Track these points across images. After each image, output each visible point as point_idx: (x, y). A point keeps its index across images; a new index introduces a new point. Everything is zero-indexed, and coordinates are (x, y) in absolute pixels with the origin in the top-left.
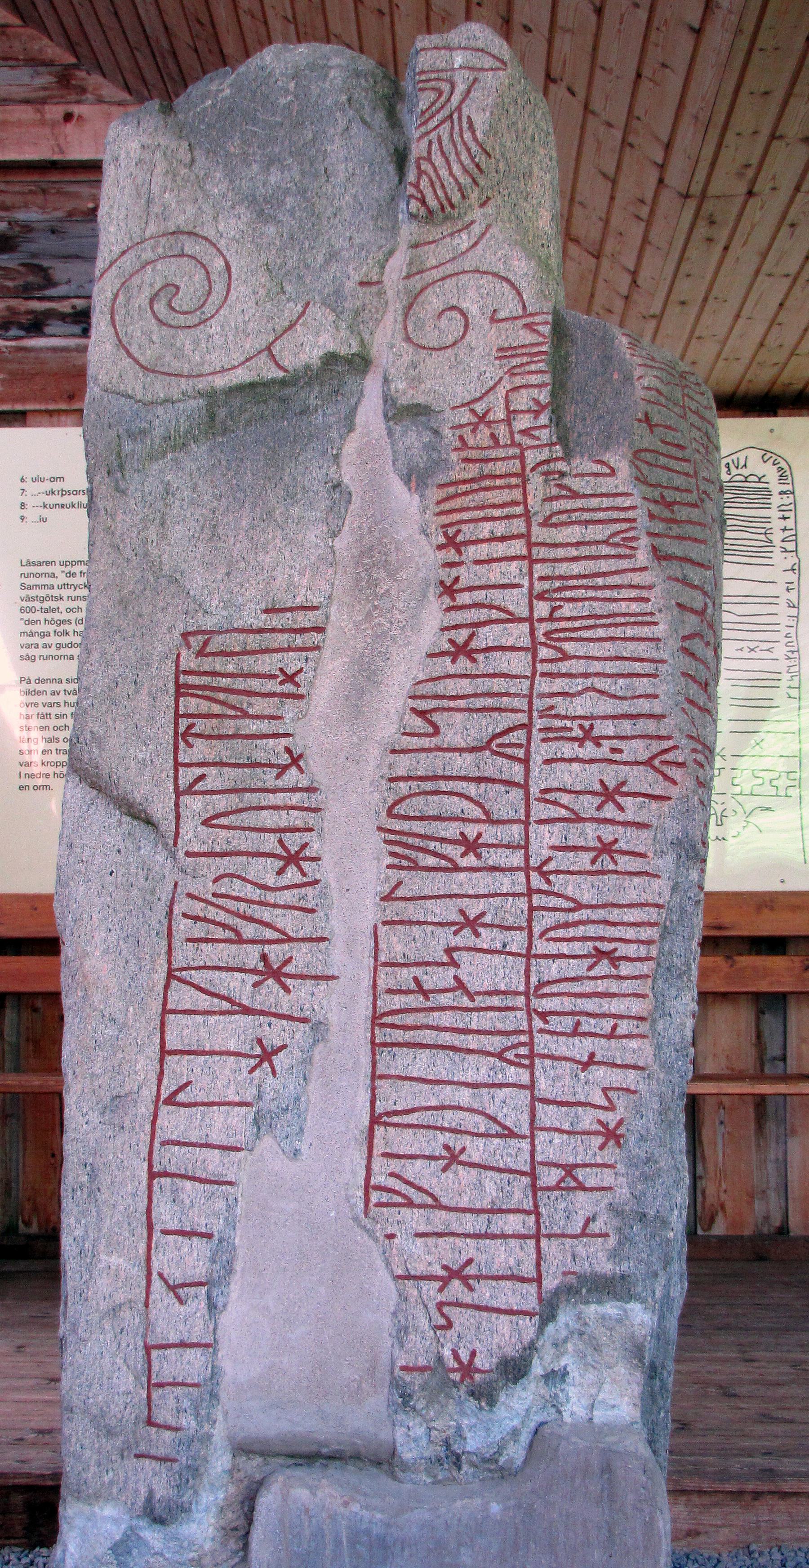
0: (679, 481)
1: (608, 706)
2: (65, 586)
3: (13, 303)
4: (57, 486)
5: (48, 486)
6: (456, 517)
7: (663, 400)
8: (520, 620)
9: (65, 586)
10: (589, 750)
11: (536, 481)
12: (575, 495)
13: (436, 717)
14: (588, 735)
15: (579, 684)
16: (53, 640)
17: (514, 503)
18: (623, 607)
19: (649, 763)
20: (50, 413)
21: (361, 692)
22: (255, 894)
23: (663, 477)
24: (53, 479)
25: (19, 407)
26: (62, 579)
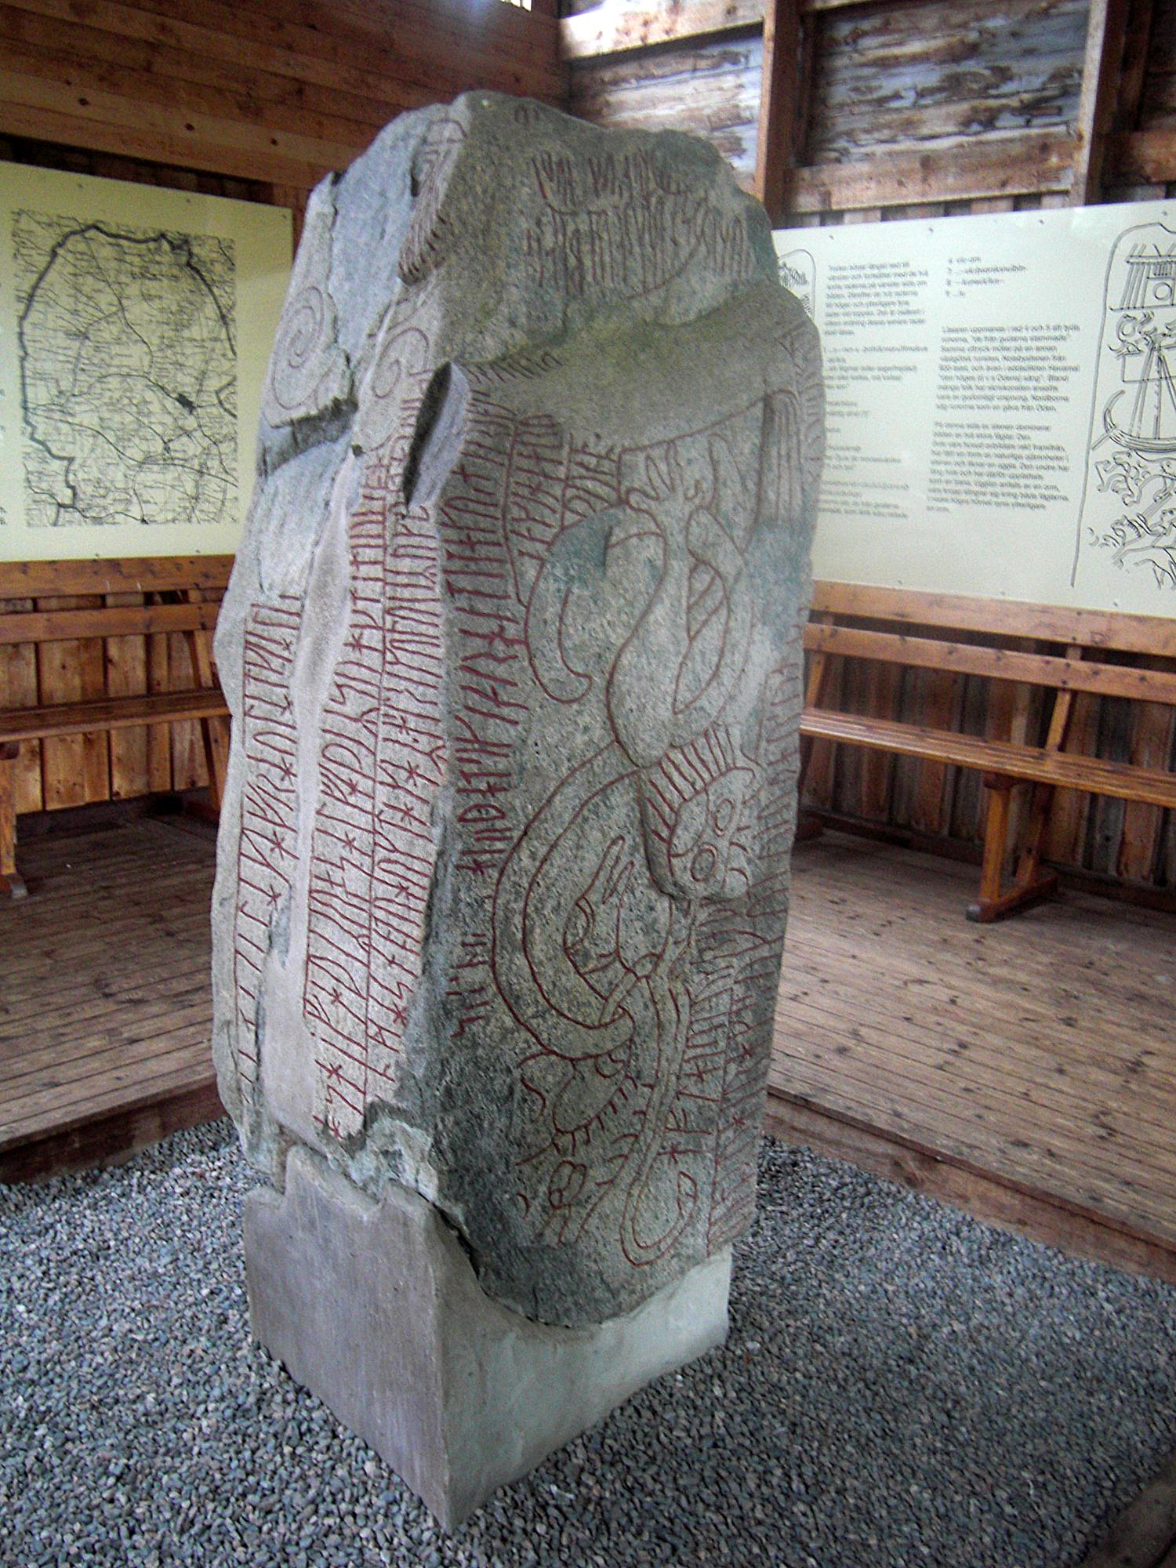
0: (484, 523)
1: (415, 707)
2: (973, 349)
3: (976, 103)
4: (974, 266)
5: (968, 265)
6: (362, 541)
7: (481, 452)
8: (377, 628)
9: (973, 349)
10: (402, 737)
11: (391, 518)
12: (410, 534)
13: (345, 690)
14: (403, 727)
15: (404, 684)
16: (961, 393)
17: (379, 536)
18: (423, 628)
19: (429, 754)
20: (989, 199)
21: (315, 664)
22: (272, 790)
23: (468, 519)
24: (973, 260)
25: (965, 196)
26: (972, 343)
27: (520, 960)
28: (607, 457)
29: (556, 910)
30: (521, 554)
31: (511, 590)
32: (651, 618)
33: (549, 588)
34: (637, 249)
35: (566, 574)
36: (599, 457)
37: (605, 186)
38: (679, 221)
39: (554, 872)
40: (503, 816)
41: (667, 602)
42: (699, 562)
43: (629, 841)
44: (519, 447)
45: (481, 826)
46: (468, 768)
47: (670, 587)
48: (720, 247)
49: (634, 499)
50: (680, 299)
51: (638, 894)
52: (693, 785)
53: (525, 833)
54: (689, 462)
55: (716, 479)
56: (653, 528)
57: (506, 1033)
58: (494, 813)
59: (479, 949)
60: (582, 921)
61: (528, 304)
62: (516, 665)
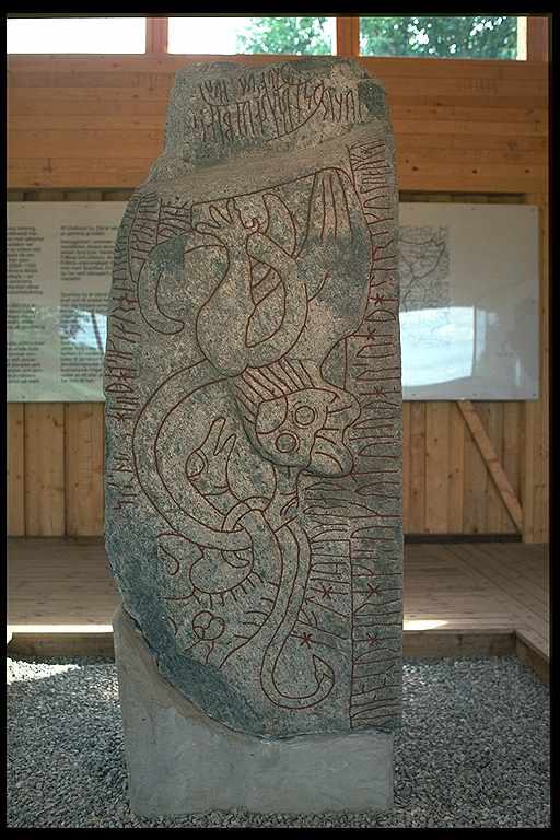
27: (154, 475)
28: (183, 207)
29: (177, 450)
30: (133, 257)
31: (128, 274)
32: (221, 291)
33: (147, 273)
34: (270, 116)
35: (159, 266)
36: (178, 208)
37: (249, 90)
38: (301, 97)
39: (172, 428)
40: (132, 391)
41: (233, 284)
42: (257, 261)
43: (229, 421)
44: (140, 209)
45: (118, 395)
46: (110, 364)
47: (235, 275)
48: (337, 106)
49: (198, 228)
50: (304, 137)
51: (242, 454)
52: (273, 392)
53: (148, 403)
54: (247, 208)
55: (269, 217)
56: (217, 242)
57: (149, 517)
58: (124, 388)
59: (125, 462)
60: (199, 463)
61: (196, 151)
62: (133, 312)
